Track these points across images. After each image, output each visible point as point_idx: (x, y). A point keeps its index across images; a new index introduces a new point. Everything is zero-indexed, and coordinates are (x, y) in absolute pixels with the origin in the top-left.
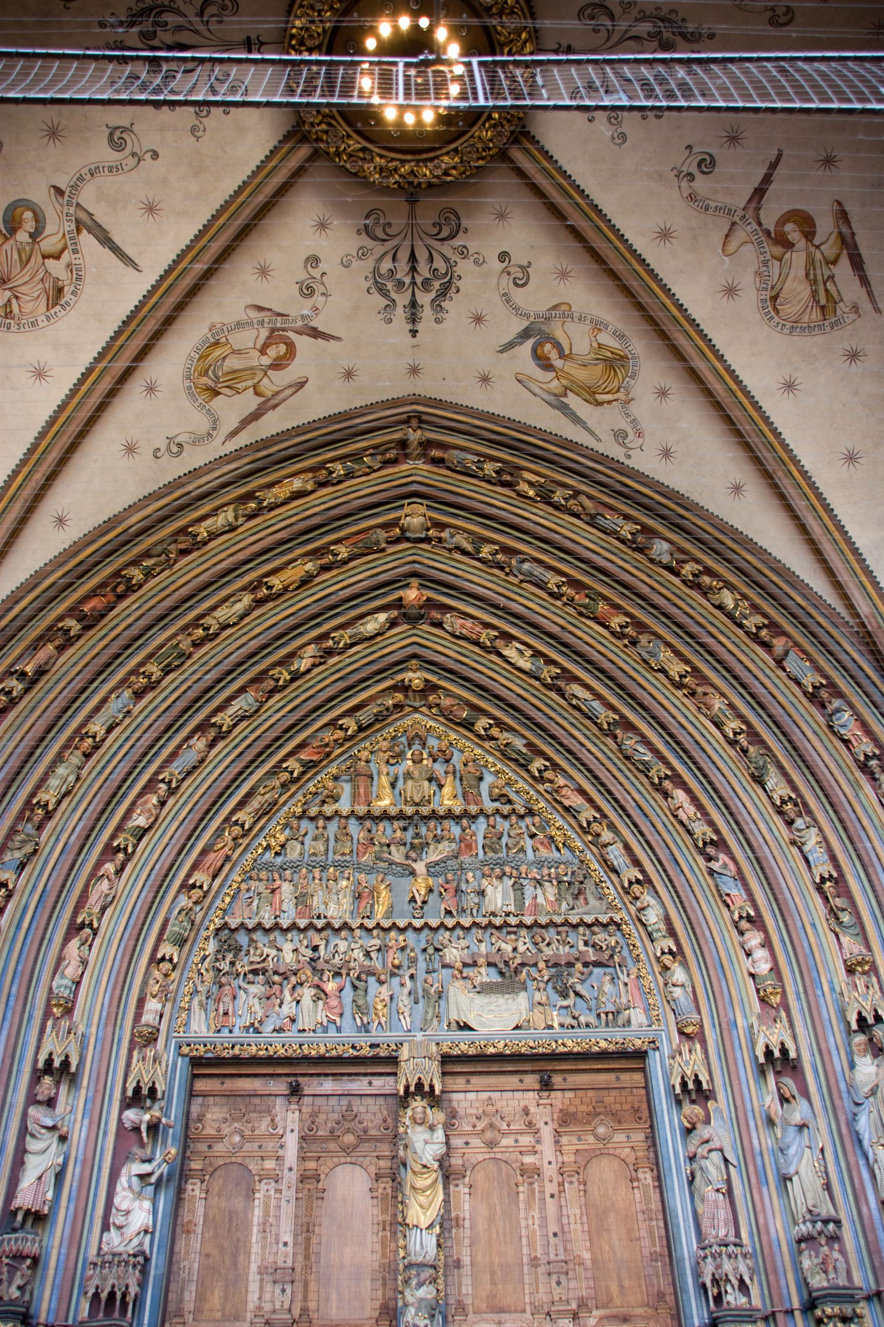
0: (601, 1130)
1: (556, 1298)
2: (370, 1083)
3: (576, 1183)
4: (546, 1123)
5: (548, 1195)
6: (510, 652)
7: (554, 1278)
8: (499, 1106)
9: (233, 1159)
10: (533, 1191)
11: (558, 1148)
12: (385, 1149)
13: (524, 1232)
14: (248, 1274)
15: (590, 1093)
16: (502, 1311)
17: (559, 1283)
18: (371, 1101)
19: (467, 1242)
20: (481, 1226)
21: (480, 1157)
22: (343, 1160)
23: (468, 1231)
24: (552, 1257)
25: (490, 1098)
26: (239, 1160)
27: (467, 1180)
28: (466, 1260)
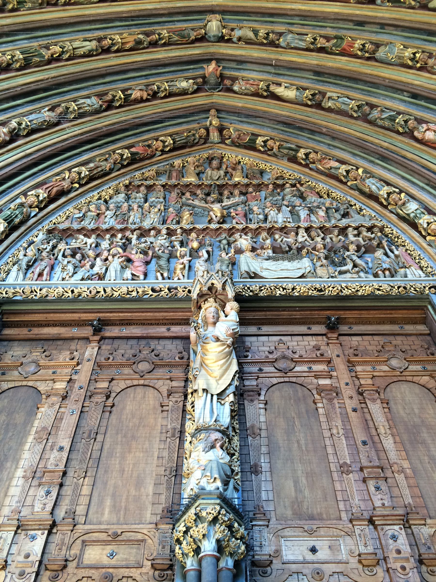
0: (394, 363)
1: (378, 503)
2: (169, 330)
3: (379, 401)
4: (338, 356)
5: (349, 410)
6: (280, 91)
7: (371, 484)
8: (289, 344)
9: (24, 383)
10: (334, 407)
11: (353, 374)
12: (178, 373)
13: (328, 442)
14: (11, 479)
15: (376, 338)
16: (312, 518)
17: (378, 488)
18: (168, 343)
19: (264, 449)
20: (280, 436)
21: (275, 381)
22: (136, 382)
23: (264, 441)
24: (365, 463)
25: (281, 340)
26: (30, 383)
27: (262, 398)
28: (265, 466)
